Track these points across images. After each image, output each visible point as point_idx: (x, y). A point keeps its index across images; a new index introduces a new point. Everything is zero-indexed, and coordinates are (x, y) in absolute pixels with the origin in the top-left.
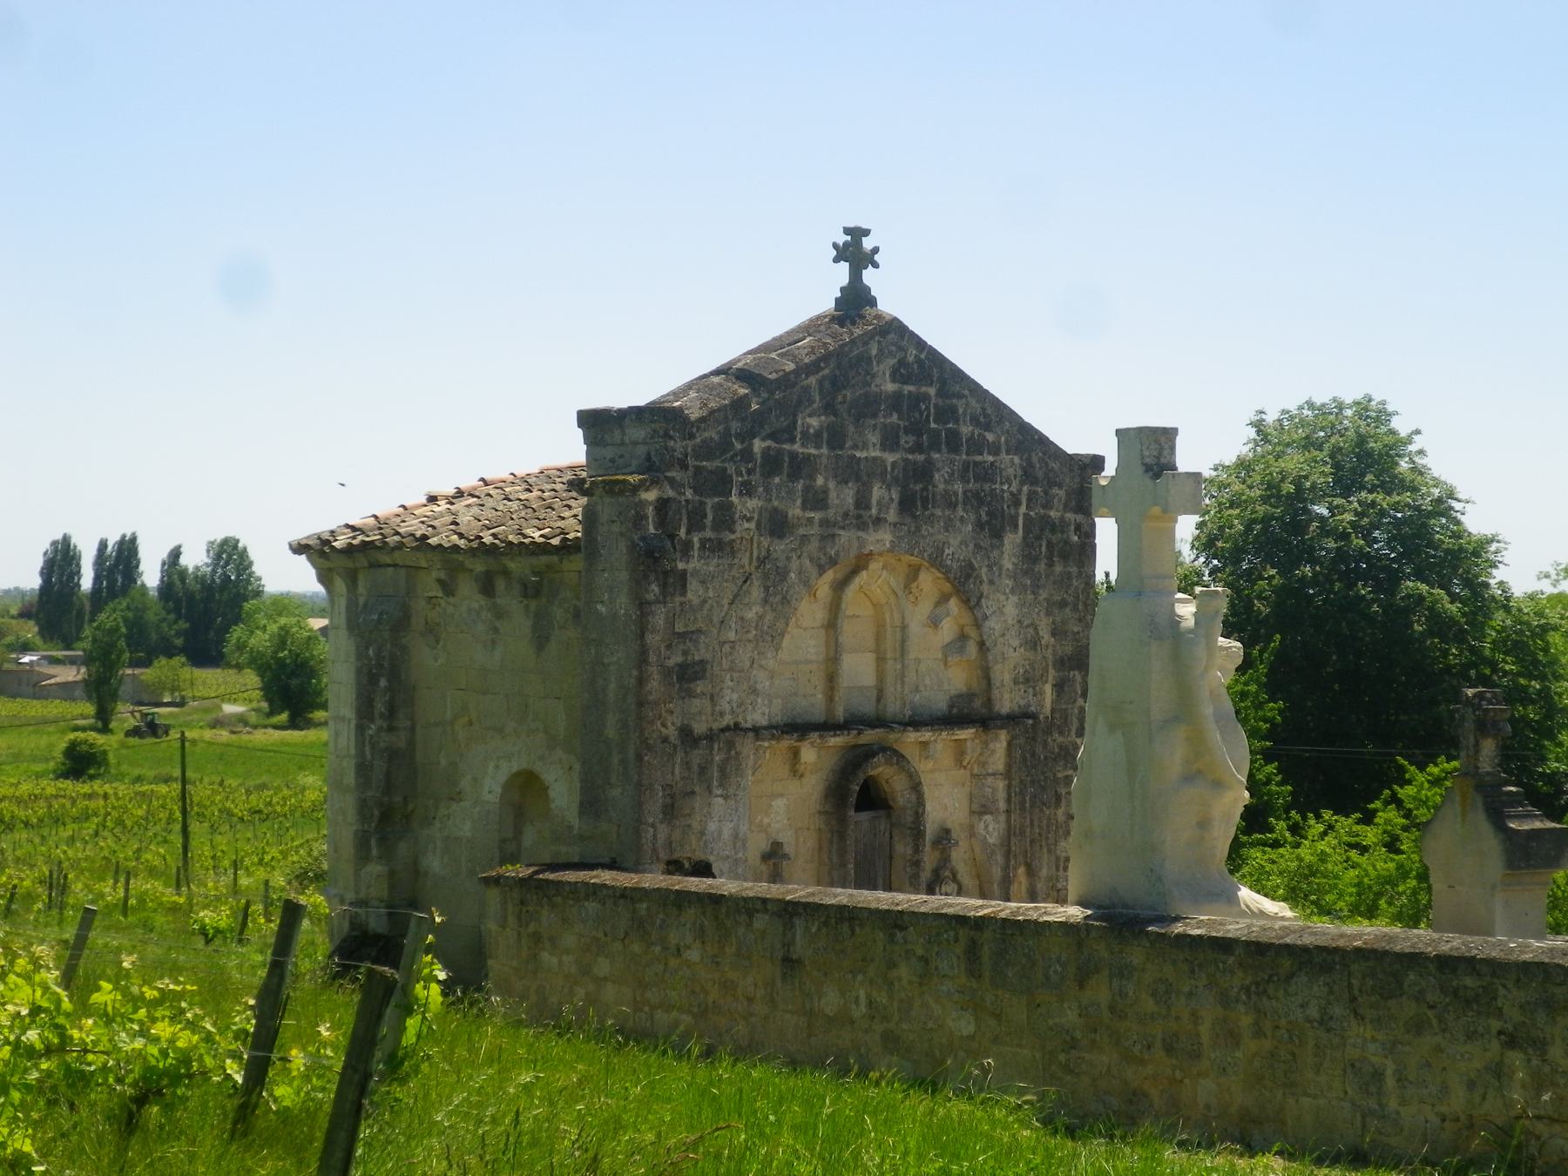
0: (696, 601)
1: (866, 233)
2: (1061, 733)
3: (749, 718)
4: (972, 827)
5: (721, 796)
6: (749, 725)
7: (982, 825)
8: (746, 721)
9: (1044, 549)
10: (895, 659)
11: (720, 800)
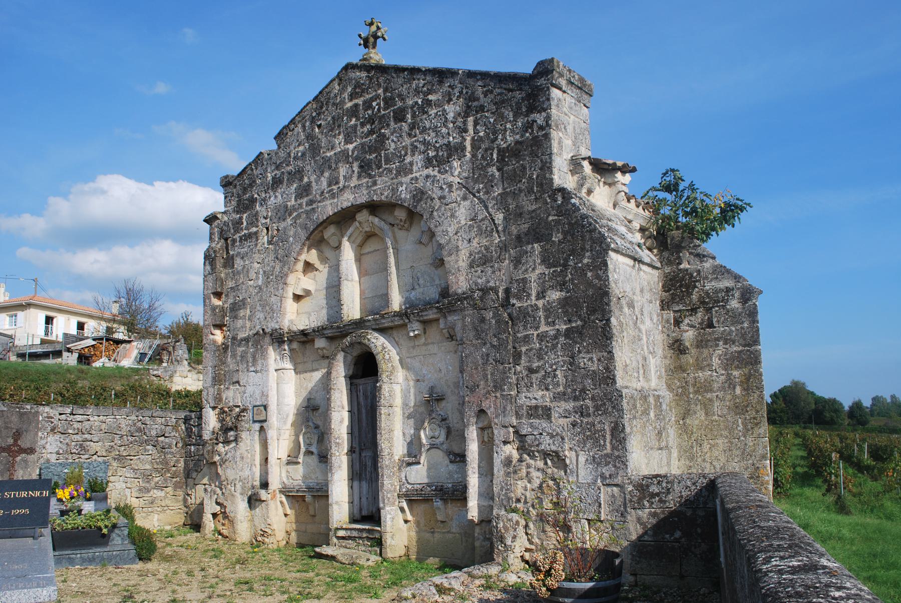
0: (240, 268)
2: (519, 298)
3: (269, 326)
8: (268, 328)
9: (495, 156)
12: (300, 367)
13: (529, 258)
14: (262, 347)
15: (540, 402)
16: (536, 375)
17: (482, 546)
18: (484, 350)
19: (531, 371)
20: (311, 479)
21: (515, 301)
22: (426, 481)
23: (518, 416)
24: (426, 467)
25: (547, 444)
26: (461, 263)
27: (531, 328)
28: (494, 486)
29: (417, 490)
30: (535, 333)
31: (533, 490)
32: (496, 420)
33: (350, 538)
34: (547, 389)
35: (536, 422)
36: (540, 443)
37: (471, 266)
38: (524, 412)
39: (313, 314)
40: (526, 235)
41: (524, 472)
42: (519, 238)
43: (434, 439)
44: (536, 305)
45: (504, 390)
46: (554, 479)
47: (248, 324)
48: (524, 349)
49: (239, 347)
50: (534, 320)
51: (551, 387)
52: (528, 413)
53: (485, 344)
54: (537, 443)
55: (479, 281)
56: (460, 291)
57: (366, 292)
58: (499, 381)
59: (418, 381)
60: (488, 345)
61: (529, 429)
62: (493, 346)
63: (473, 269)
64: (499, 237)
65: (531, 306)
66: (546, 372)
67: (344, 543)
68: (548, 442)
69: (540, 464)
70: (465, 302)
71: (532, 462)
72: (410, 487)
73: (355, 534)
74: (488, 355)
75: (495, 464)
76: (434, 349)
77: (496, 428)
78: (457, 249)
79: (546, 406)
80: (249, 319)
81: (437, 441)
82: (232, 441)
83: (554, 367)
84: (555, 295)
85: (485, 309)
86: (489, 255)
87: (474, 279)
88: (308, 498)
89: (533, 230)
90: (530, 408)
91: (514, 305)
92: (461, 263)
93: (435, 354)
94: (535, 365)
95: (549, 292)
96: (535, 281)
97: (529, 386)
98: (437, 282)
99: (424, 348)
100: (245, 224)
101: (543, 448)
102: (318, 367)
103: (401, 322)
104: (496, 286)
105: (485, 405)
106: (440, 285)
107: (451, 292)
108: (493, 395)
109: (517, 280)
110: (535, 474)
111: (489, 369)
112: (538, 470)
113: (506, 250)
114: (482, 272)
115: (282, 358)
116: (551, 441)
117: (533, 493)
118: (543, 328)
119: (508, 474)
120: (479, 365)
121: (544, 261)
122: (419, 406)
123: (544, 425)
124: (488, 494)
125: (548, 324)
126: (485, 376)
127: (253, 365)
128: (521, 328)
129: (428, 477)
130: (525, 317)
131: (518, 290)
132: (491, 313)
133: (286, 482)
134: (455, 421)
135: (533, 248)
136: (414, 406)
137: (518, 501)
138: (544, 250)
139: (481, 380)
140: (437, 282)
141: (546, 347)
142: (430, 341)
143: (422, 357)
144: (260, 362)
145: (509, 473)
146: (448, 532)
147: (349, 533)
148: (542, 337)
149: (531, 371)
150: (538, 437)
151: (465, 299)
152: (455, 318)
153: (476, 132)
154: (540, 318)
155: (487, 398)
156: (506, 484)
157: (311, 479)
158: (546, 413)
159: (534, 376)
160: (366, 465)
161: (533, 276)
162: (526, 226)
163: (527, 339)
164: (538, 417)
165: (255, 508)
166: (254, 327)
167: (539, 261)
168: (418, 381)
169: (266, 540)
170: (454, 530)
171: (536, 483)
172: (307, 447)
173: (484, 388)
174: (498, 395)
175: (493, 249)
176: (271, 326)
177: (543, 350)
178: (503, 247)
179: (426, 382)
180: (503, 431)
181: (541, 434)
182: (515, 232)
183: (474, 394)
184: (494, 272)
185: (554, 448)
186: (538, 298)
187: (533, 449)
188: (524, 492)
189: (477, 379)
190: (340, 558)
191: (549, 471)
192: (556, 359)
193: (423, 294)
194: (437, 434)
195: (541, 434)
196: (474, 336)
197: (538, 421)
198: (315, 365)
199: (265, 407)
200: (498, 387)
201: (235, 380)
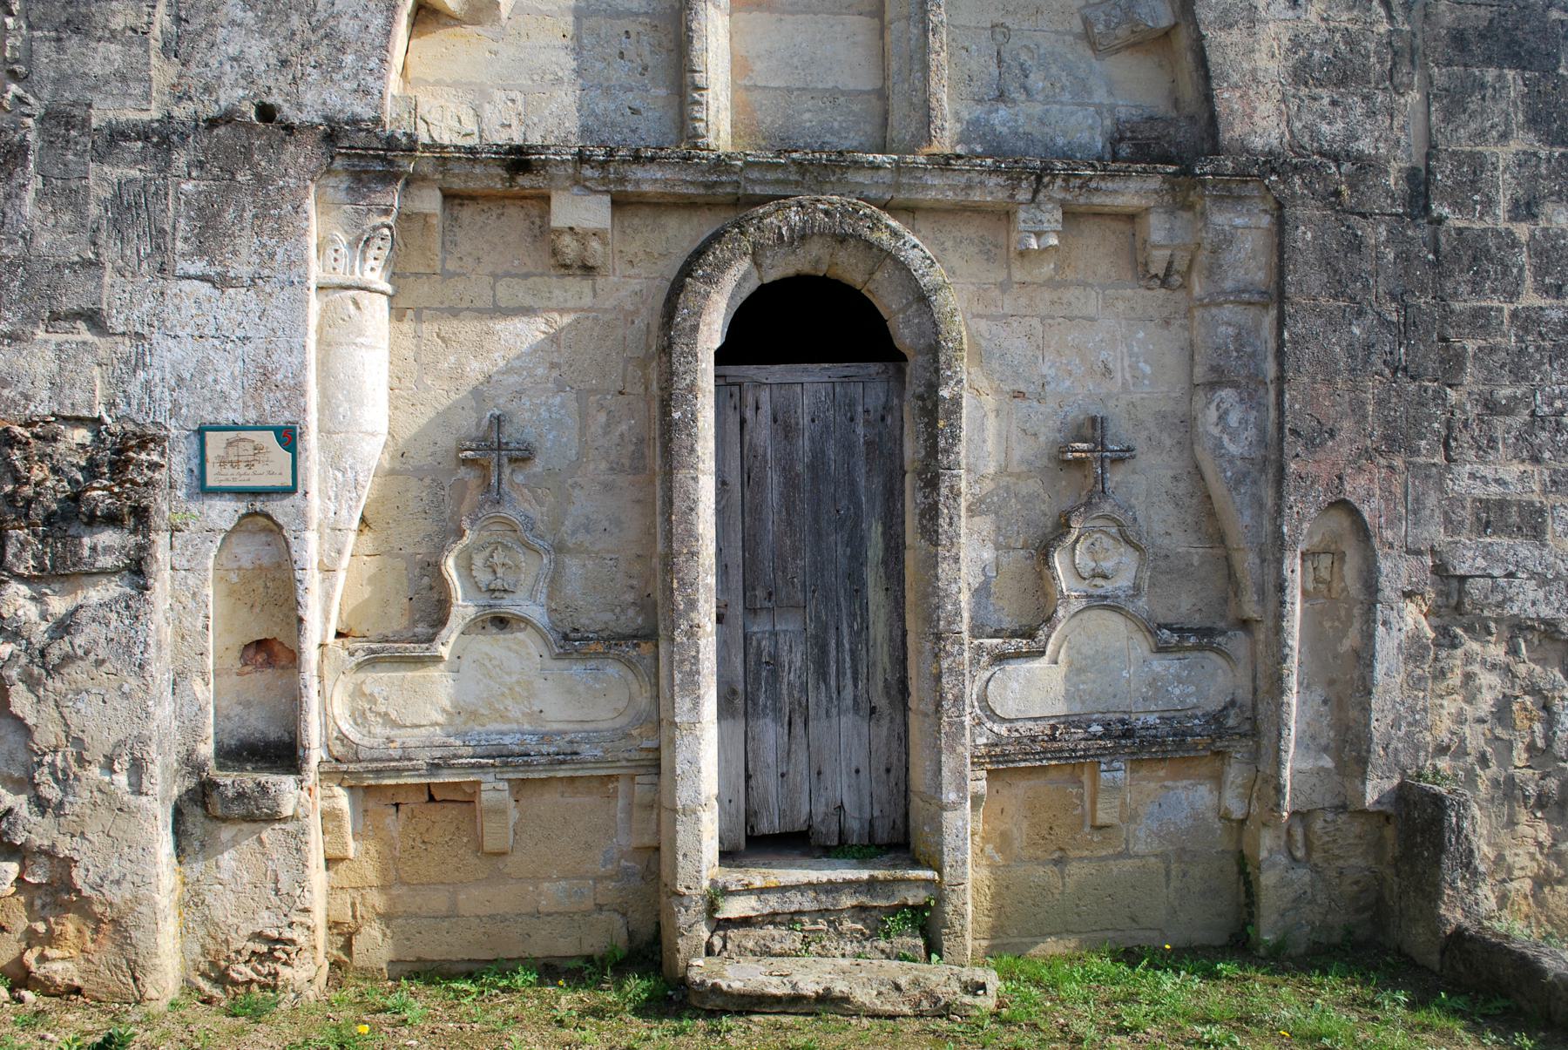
2: (1458, 206)
3: (309, 97)
4: (1188, 423)
5: (203, 278)
6: (310, 115)
7: (1213, 414)
8: (300, 107)
10: (909, 18)
11: (206, 288)
12: (421, 291)
13: (1489, 103)
14: (261, 180)
15: (1514, 492)
16: (1509, 420)
17: (1283, 883)
18: (1356, 331)
19: (1491, 407)
20: (504, 718)
21: (1446, 211)
22: (1061, 709)
23: (1451, 525)
24: (1062, 668)
26: (1262, 60)
27: (1494, 291)
28: (1374, 716)
29: (1033, 739)
30: (1507, 308)
31: (1481, 721)
32: (1388, 534)
33: (772, 918)
34: (1536, 460)
35: (1501, 543)
36: (1504, 601)
37: (1301, 74)
38: (1467, 514)
39: (499, 95)
40: (1482, 36)
41: (1455, 679)
42: (1459, 39)
43: (1099, 581)
44: (1510, 233)
45: (1417, 452)
46: (1534, 690)
47: (162, 72)
48: (1471, 346)
49: (101, 158)
50: (1504, 274)
51: (1547, 455)
52: (1479, 519)
53: (1361, 313)
54: (1500, 597)
55: (1324, 128)
56: (1258, 143)
57: (759, 66)
58: (1402, 423)
59: (1019, 395)
60: (1371, 317)
61: (1480, 562)
62: (1385, 323)
63: (1304, 91)
64: (1391, 18)
65: (1497, 234)
66: (1533, 414)
67: (751, 938)
68: (1531, 595)
69: (1497, 652)
70: (1297, 180)
71: (1475, 646)
72: (1002, 730)
73: (806, 902)
74: (1369, 347)
75: (1380, 655)
76: (1090, 303)
77: (1386, 556)
78: (1252, 19)
79: (1531, 504)
80: (165, 49)
81: (1108, 587)
82: (103, 572)
83: (1558, 404)
85: (1363, 216)
86: (1358, 61)
87: (1307, 118)
88: (494, 790)
89: (1506, 30)
90: (1485, 504)
91: (1440, 220)
92: (1262, 60)
93: (1092, 319)
94: (1504, 393)
95: (1548, 208)
96: (1507, 168)
98: (1100, 96)
99: (1048, 295)
101: (1516, 610)
102: (528, 301)
103: (1002, 195)
104: (1377, 157)
105: (1354, 488)
106: (1112, 109)
107: (1226, 137)
108: (1383, 462)
109: (1454, 153)
110: (1486, 679)
111: (1371, 388)
112: (1494, 666)
113: (1412, 62)
114: (1334, 103)
115: (362, 243)
116: (1541, 594)
117: (1479, 728)
118: (1530, 299)
119: (1416, 683)
120: (1338, 372)
121: (1534, 121)
122: (1018, 476)
123: (1523, 552)
124: (1313, 738)
125: (1545, 290)
126: (1358, 407)
127: (201, 251)
128: (1464, 289)
129: (1069, 697)
130: (1475, 259)
131: (1458, 183)
132: (1382, 230)
133: (354, 735)
134: (1158, 528)
135: (1501, 77)
136: (1002, 471)
137: (1442, 750)
138: (1533, 93)
139: (1343, 415)
140: (1100, 96)
141: (1538, 348)
142: (1070, 275)
143: (1036, 322)
144: (247, 244)
145: (1420, 679)
146: (1124, 855)
147: (773, 903)
148: (1527, 321)
149: (1491, 407)
150: (1502, 582)
151: (1296, 168)
152: (1238, 221)
154: (1521, 269)
155: (1360, 469)
156: (1412, 710)
157: (504, 718)
159: (1500, 422)
160: (774, 664)
161: (1504, 154)
162: (1482, 11)
163: (1481, 321)
164: (1505, 529)
165: (208, 848)
166: (207, 89)
167: (1521, 118)
168: (1019, 395)
169: (285, 972)
170: (1140, 848)
171: (1486, 703)
172: (485, 599)
173: (1352, 441)
174: (1398, 462)
175: (1372, 47)
177: (1531, 356)
178: (1402, 53)
179: (1051, 403)
180: (1407, 565)
181: (1511, 575)
182: (1448, 19)
183: (1320, 455)
184: (1371, 114)
185: (1546, 612)
186: (1515, 216)
187: (1486, 613)
188: (1454, 727)
189: (1332, 412)
190: (864, 996)
191: (1521, 669)
193: (1042, 122)
194: (1107, 565)
195: (1511, 575)
196: (1323, 286)
197: (1505, 541)
198: (506, 293)
199: (289, 437)
200: (1397, 440)
201: (67, 303)
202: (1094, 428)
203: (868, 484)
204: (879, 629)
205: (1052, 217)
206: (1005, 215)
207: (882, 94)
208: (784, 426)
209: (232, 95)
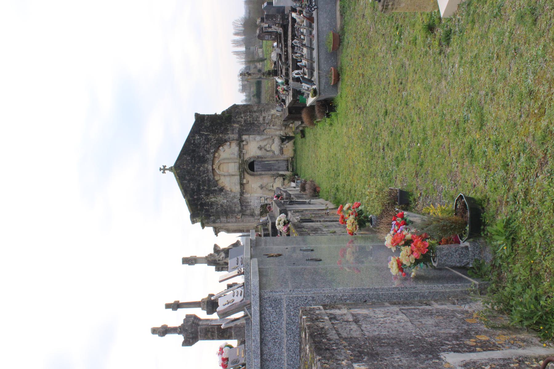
1: (160, 168)
4: (258, 141)
23: (265, 123)
25: (270, 117)
84: (242, 115)
97: (259, 121)
100: (207, 207)
118: (248, 117)
148: (250, 118)
153: (204, 131)
158: (264, 117)
163: (250, 121)
176: (238, 196)
192: (255, 115)
202: (258, 148)
203: (263, 163)
204: (273, 162)
205: (244, 151)
206: (243, 154)
207: (235, 162)
208: (259, 168)
209: (239, 201)
